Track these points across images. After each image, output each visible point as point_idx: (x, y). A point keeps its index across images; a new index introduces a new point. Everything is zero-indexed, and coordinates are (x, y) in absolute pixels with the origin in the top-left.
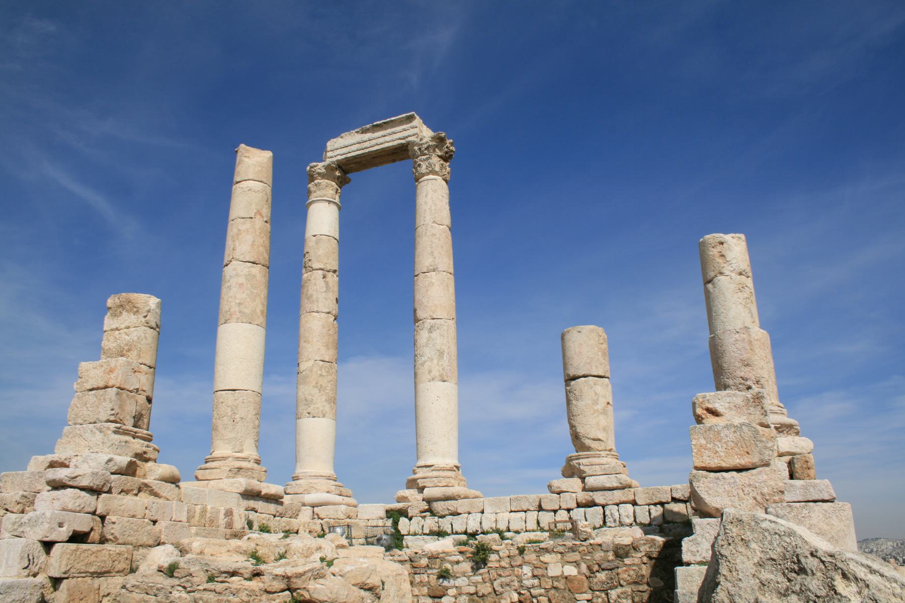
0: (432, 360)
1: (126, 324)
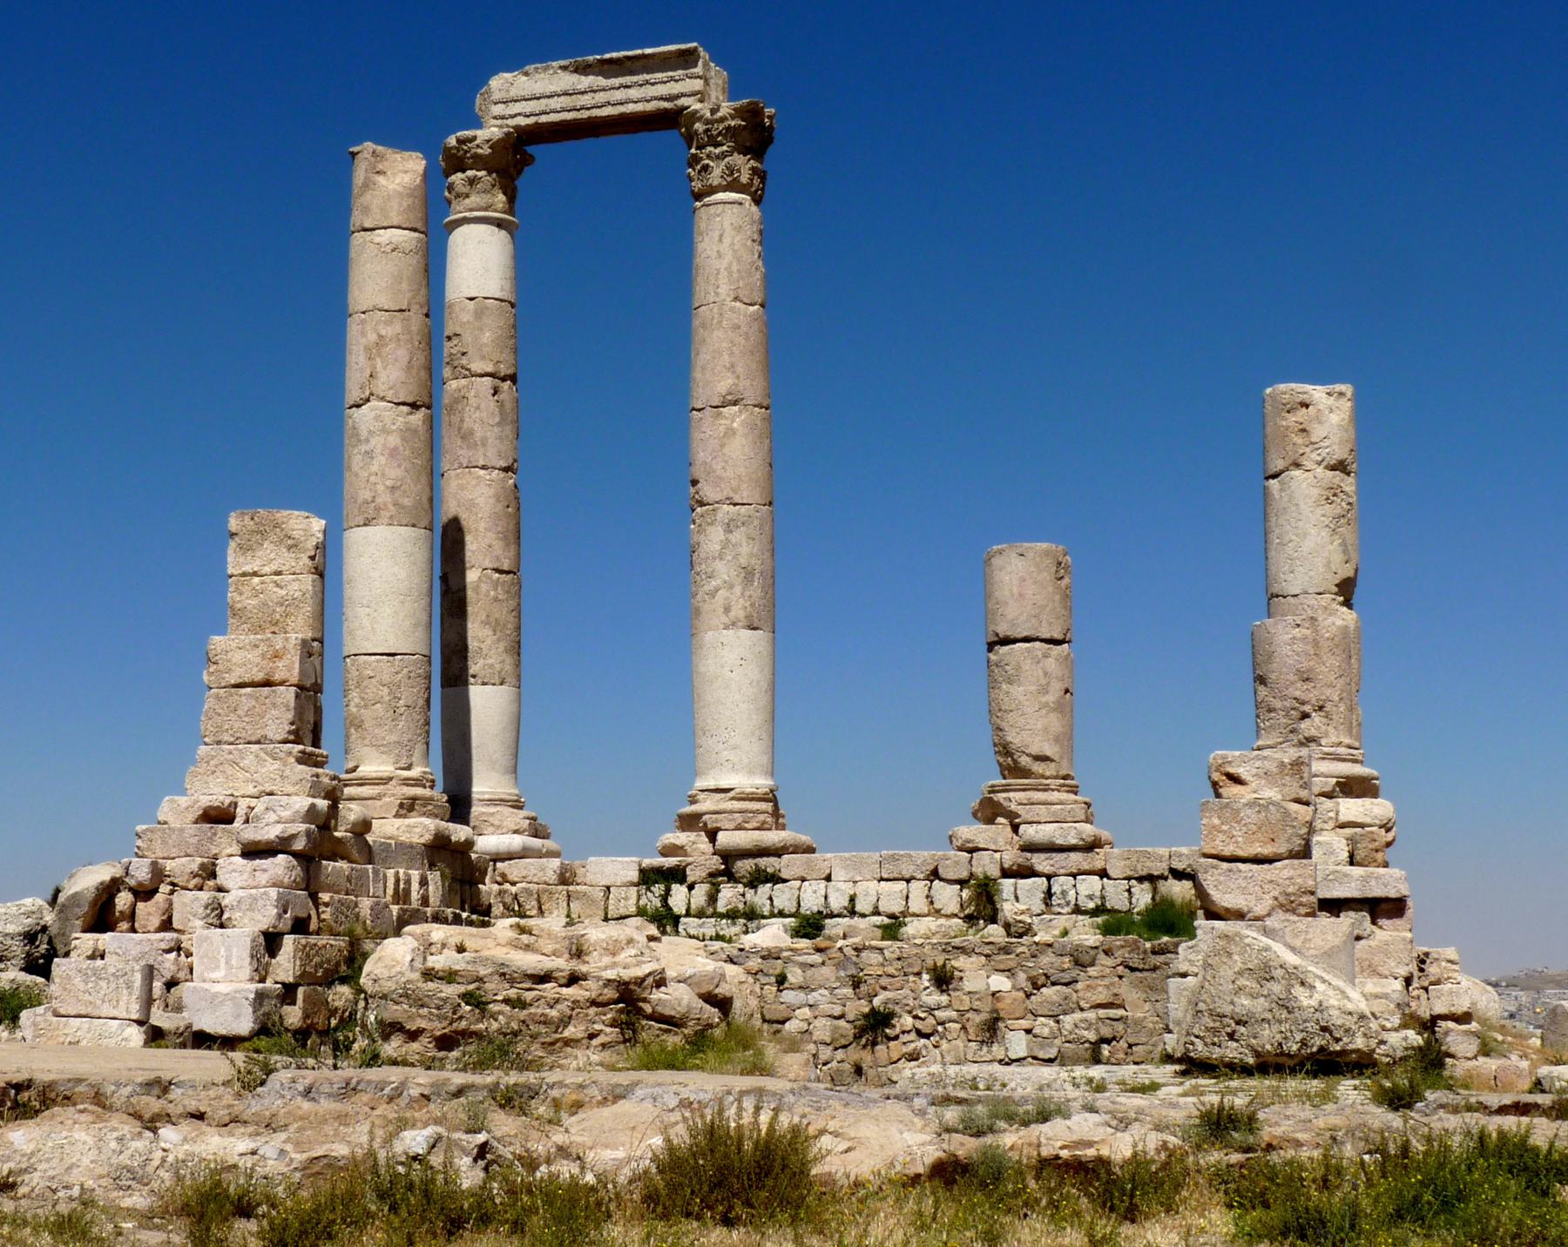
0: (731, 587)
1: (274, 567)
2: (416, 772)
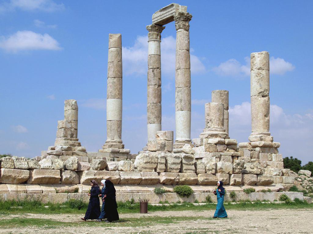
2: (115, 140)
